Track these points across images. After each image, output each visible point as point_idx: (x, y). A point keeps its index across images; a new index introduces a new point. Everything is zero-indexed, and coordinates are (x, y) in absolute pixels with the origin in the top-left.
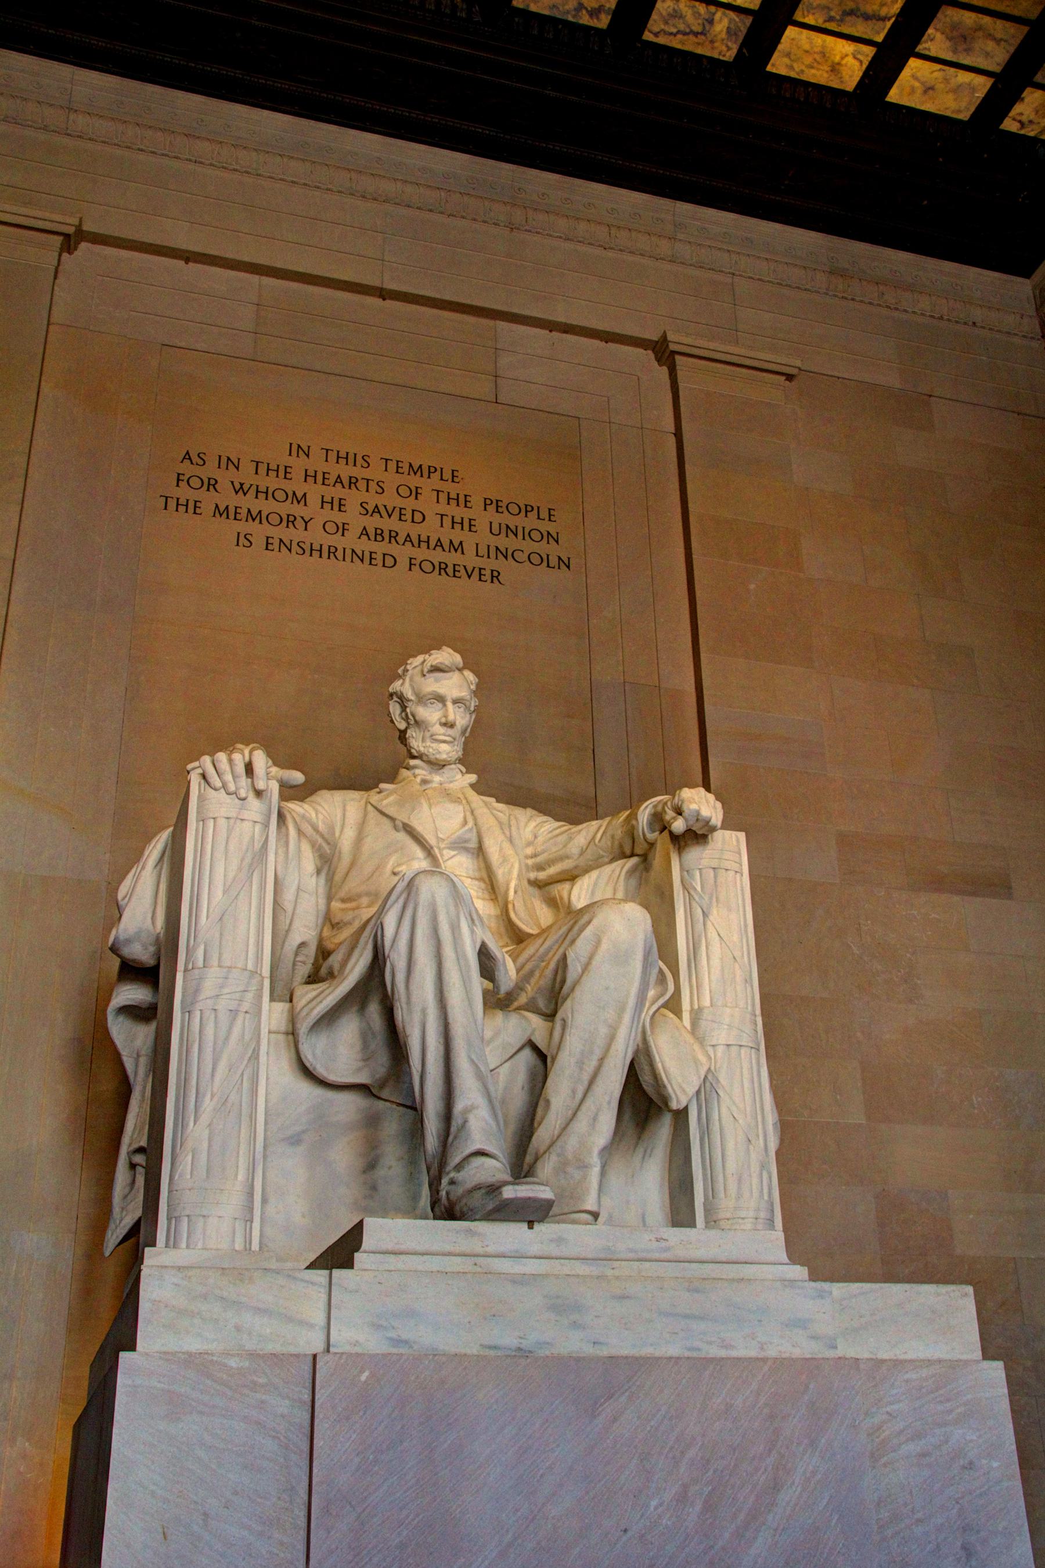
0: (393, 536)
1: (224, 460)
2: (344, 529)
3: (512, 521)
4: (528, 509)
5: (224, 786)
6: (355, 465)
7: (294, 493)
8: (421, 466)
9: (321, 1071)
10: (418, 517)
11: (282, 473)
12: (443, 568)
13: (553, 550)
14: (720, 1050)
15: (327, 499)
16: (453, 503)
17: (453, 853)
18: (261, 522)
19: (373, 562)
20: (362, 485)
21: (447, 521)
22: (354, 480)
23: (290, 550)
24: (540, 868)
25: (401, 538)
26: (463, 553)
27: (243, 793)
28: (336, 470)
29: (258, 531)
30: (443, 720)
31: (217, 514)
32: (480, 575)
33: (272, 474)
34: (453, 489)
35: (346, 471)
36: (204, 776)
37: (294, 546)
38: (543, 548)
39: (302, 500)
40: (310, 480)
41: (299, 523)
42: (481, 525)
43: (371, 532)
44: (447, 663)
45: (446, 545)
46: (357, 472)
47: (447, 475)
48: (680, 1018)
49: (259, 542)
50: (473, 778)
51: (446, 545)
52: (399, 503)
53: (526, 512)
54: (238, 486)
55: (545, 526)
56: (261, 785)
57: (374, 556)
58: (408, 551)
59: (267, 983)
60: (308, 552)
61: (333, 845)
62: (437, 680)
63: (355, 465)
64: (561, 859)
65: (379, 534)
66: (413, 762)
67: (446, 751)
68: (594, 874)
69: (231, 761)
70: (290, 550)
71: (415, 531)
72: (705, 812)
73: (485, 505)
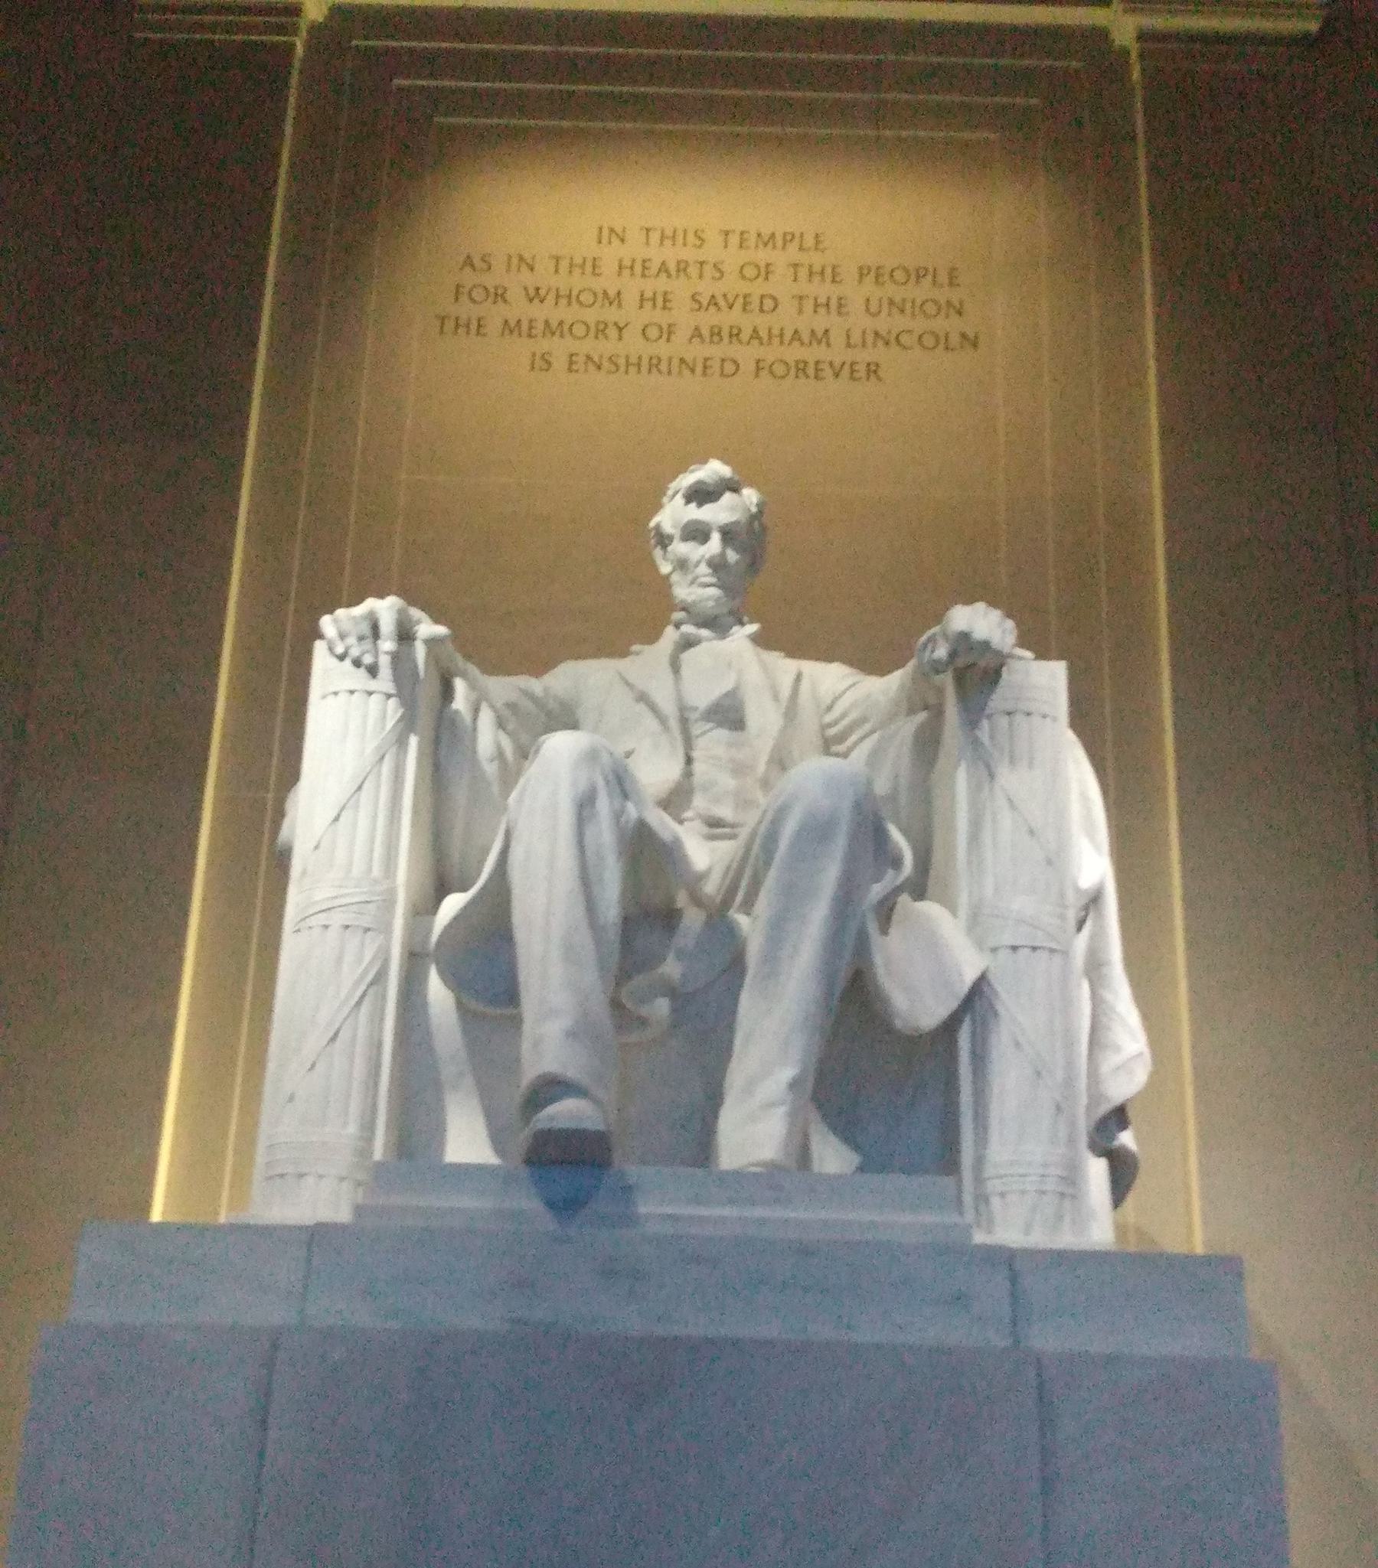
0: (735, 335)
1: (515, 261)
2: (670, 333)
3: (898, 293)
4: (920, 274)
6: (685, 245)
7: (605, 293)
8: (773, 235)
10: (768, 304)
11: (589, 268)
13: (952, 325)
14: (1003, 955)
15: (649, 294)
16: (817, 279)
17: (710, 725)
18: (562, 336)
19: (709, 371)
20: (693, 271)
21: (809, 306)
22: (682, 266)
23: (599, 368)
25: (745, 336)
26: (828, 345)
27: (368, 659)
28: (657, 255)
29: (559, 348)
30: (707, 556)
31: (507, 332)
32: (852, 371)
33: (577, 271)
34: (817, 260)
35: (670, 255)
37: (606, 364)
38: (940, 324)
39: (615, 299)
40: (626, 272)
42: (856, 305)
43: (706, 333)
45: (806, 338)
46: (689, 254)
47: (809, 241)
49: (560, 363)
50: (752, 628)
51: (806, 338)
52: (744, 288)
53: (918, 277)
54: (532, 292)
55: (943, 295)
57: (709, 363)
58: (755, 351)
60: (622, 369)
62: (700, 505)
63: (685, 245)
65: (716, 333)
66: (678, 615)
68: (876, 736)
70: (599, 368)
71: (762, 322)
73: (861, 275)
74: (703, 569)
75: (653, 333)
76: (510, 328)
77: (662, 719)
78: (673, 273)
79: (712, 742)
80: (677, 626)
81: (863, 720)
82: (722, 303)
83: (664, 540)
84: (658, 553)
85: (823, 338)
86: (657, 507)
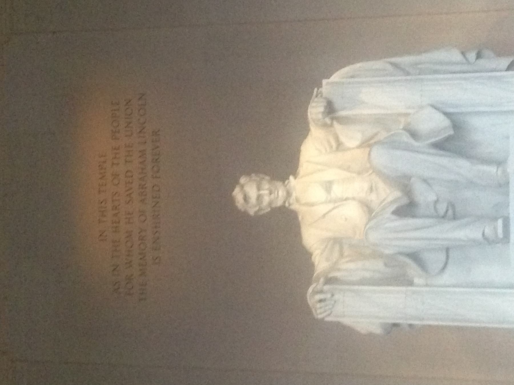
5: (330, 309)
9: (441, 265)
12: (156, 161)
24: (331, 147)
27: (333, 302)
36: (326, 316)
39: (129, 235)
41: (143, 234)
44: (242, 196)
48: (409, 114)
56: (329, 296)
59: (410, 288)
61: (329, 239)
62: (250, 198)
64: (329, 142)
67: (282, 193)
69: (321, 308)
72: (322, 109)
74: (272, 196)
75: (143, 218)
76: (143, 273)
77: (334, 208)
78: (116, 212)
79: (337, 191)
80: (290, 205)
81: (329, 142)
82: (130, 192)
83: (260, 210)
84: (262, 212)
85: (143, 153)
86: (245, 214)
